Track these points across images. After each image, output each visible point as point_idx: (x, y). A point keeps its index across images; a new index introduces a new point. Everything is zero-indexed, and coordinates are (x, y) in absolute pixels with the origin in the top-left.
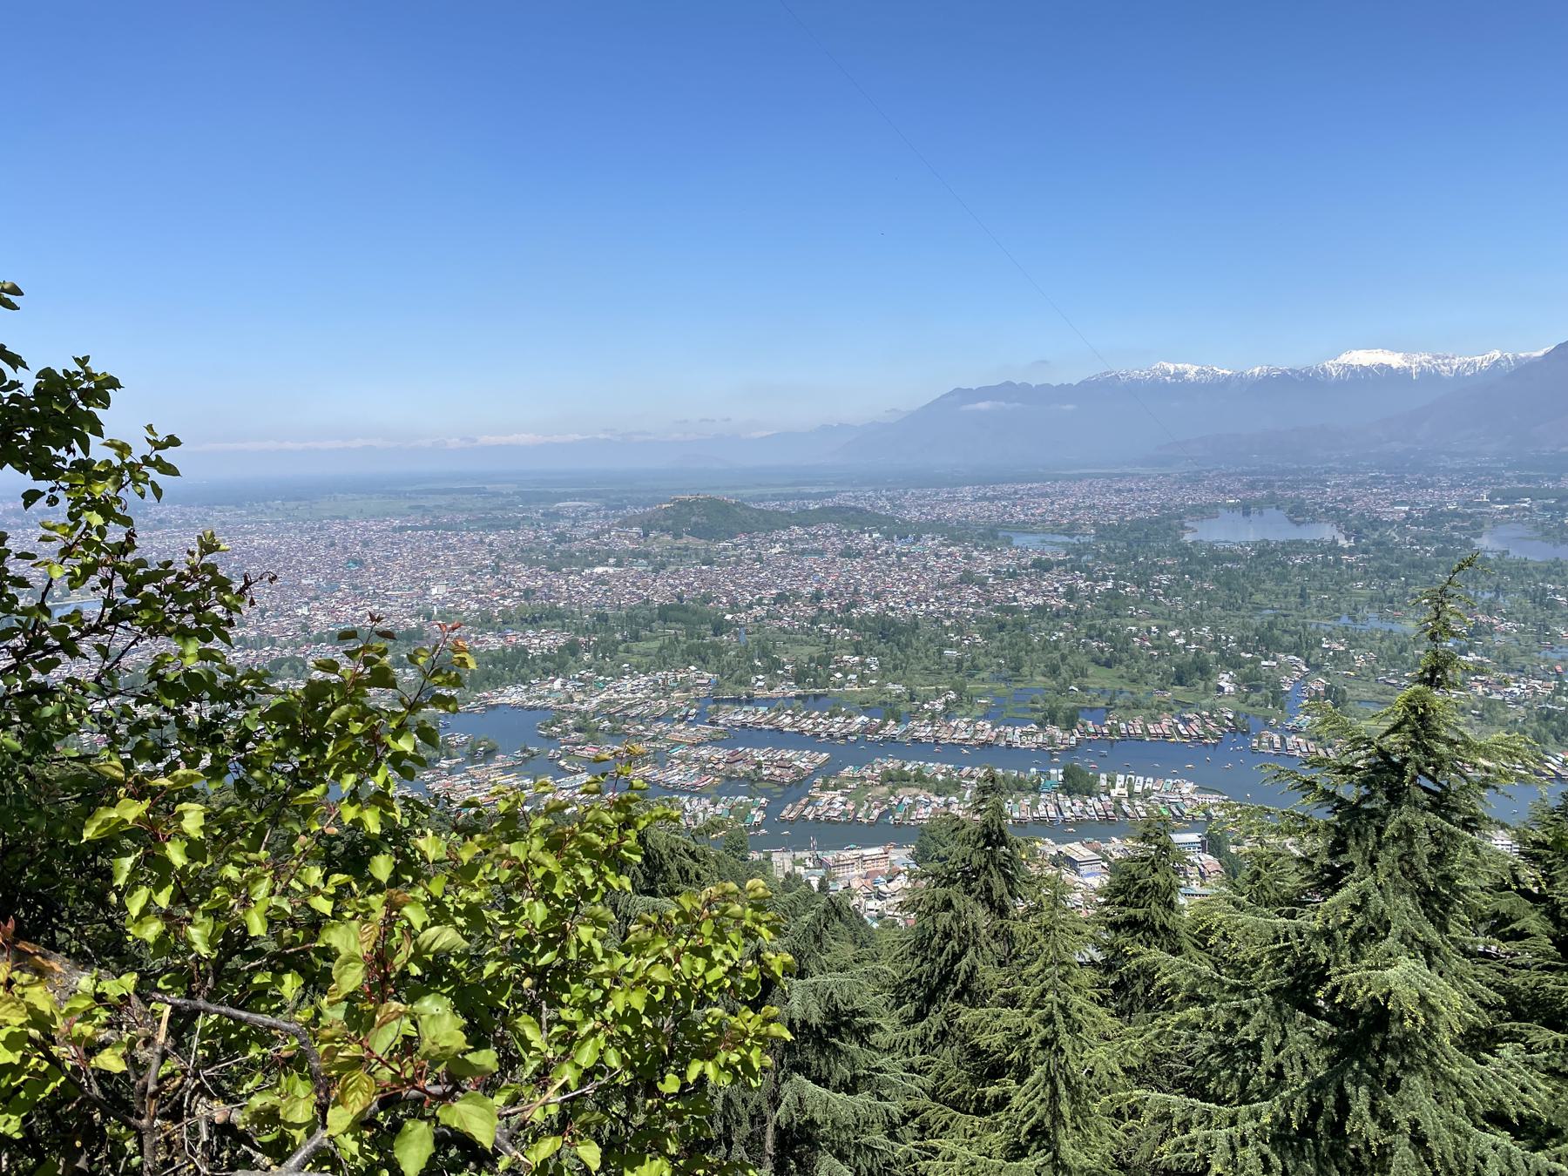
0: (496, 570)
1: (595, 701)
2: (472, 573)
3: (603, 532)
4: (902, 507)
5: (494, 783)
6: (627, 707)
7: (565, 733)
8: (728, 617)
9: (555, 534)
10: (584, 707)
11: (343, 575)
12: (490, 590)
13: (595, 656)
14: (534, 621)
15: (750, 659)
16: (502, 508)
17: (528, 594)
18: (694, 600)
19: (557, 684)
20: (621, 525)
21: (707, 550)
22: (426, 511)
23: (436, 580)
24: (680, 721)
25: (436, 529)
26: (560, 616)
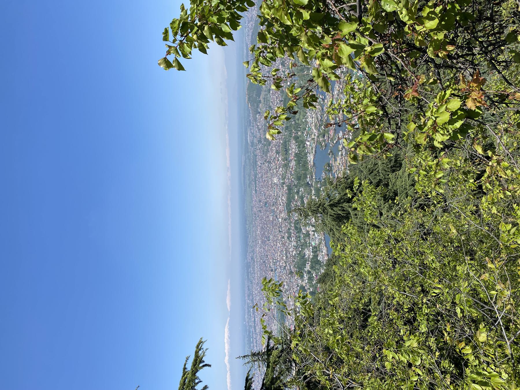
0: (269, 162)
1: (315, 131)
2: (270, 170)
3: (258, 127)
4: (252, 18)
5: (340, 164)
6: (318, 120)
7: (324, 141)
8: (289, 83)
9: (258, 143)
10: (317, 135)
11: (270, 208)
12: (276, 164)
13: (299, 131)
14: (287, 151)
15: (304, 75)
16: (250, 160)
17: (277, 152)
18: (282, 96)
19: (308, 143)
20: (256, 121)
21: (265, 91)
22: (250, 183)
23: (272, 181)
24: (324, 101)
25: (256, 181)
26: (285, 142)
